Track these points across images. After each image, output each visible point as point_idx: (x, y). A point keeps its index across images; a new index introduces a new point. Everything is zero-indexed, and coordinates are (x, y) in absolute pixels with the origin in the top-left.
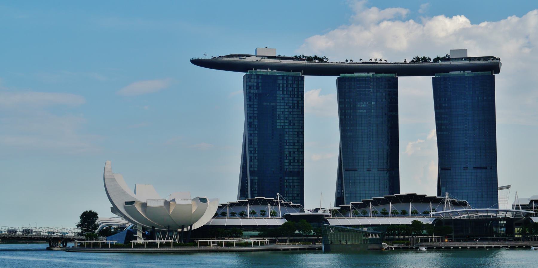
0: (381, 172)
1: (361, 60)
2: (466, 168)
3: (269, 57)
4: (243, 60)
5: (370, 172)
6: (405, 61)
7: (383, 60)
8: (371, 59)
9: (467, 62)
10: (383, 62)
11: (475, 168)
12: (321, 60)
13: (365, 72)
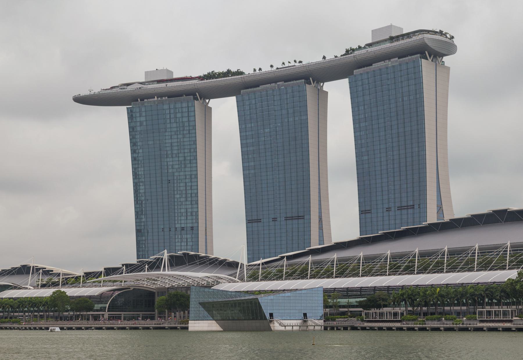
0: (289, 222)
1: (272, 66)
2: (389, 209)
3: (159, 82)
4: (124, 90)
5: (276, 222)
6: (324, 58)
7: (298, 62)
8: (283, 63)
9: (388, 45)
10: (297, 64)
11: (401, 208)
12: (239, 73)
13: (270, 83)
